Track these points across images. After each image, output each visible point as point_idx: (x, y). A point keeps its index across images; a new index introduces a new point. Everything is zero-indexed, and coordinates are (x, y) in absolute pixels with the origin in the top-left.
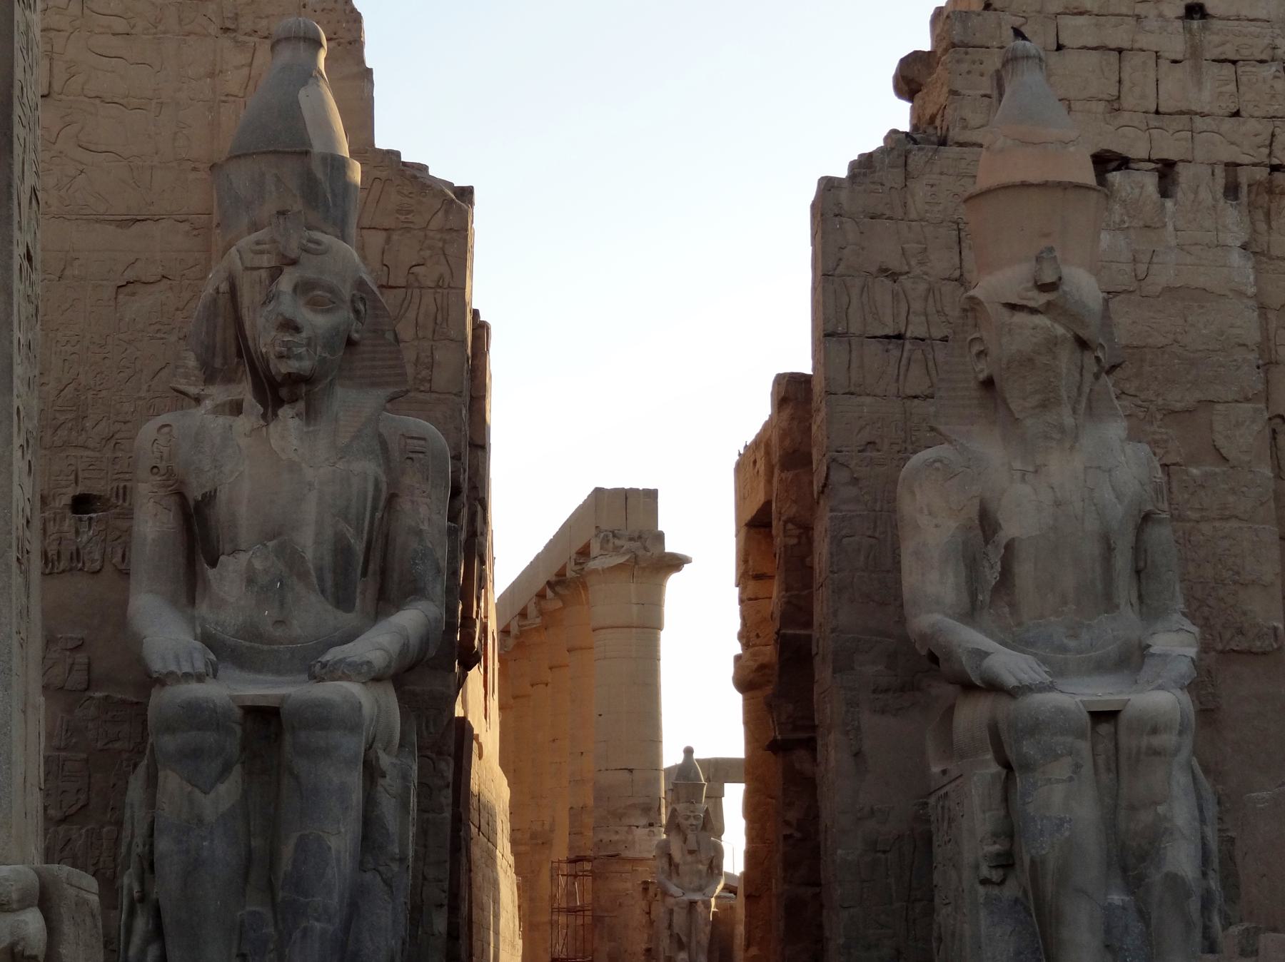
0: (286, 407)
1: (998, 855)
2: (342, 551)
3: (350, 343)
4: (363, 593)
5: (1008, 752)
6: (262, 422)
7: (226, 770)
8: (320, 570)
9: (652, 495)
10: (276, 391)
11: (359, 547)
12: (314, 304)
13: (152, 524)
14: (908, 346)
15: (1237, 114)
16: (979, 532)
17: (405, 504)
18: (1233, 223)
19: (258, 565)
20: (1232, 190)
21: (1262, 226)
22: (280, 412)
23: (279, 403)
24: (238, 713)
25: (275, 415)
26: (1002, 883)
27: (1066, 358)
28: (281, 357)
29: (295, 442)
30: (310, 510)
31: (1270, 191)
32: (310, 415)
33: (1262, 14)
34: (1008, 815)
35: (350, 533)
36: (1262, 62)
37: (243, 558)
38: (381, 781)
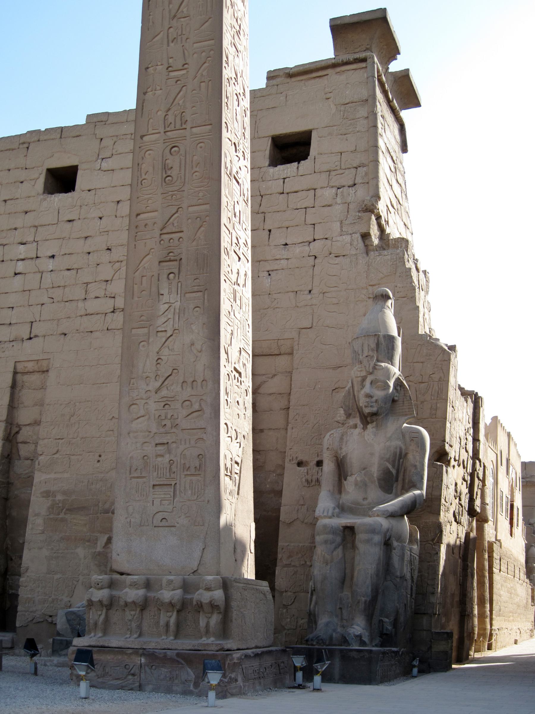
0: (370, 425)
3: (394, 401)
6: (362, 430)
7: (335, 548)
10: (367, 419)
11: (394, 472)
13: (329, 467)
17: (410, 456)
19: (358, 479)
22: (368, 426)
23: (368, 423)
24: (342, 528)
25: (367, 428)
29: (373, 436)
30: (376, 460)
32: (377, 426)
35: (390, 467)
37: (354, 477)
38: (393, 551)
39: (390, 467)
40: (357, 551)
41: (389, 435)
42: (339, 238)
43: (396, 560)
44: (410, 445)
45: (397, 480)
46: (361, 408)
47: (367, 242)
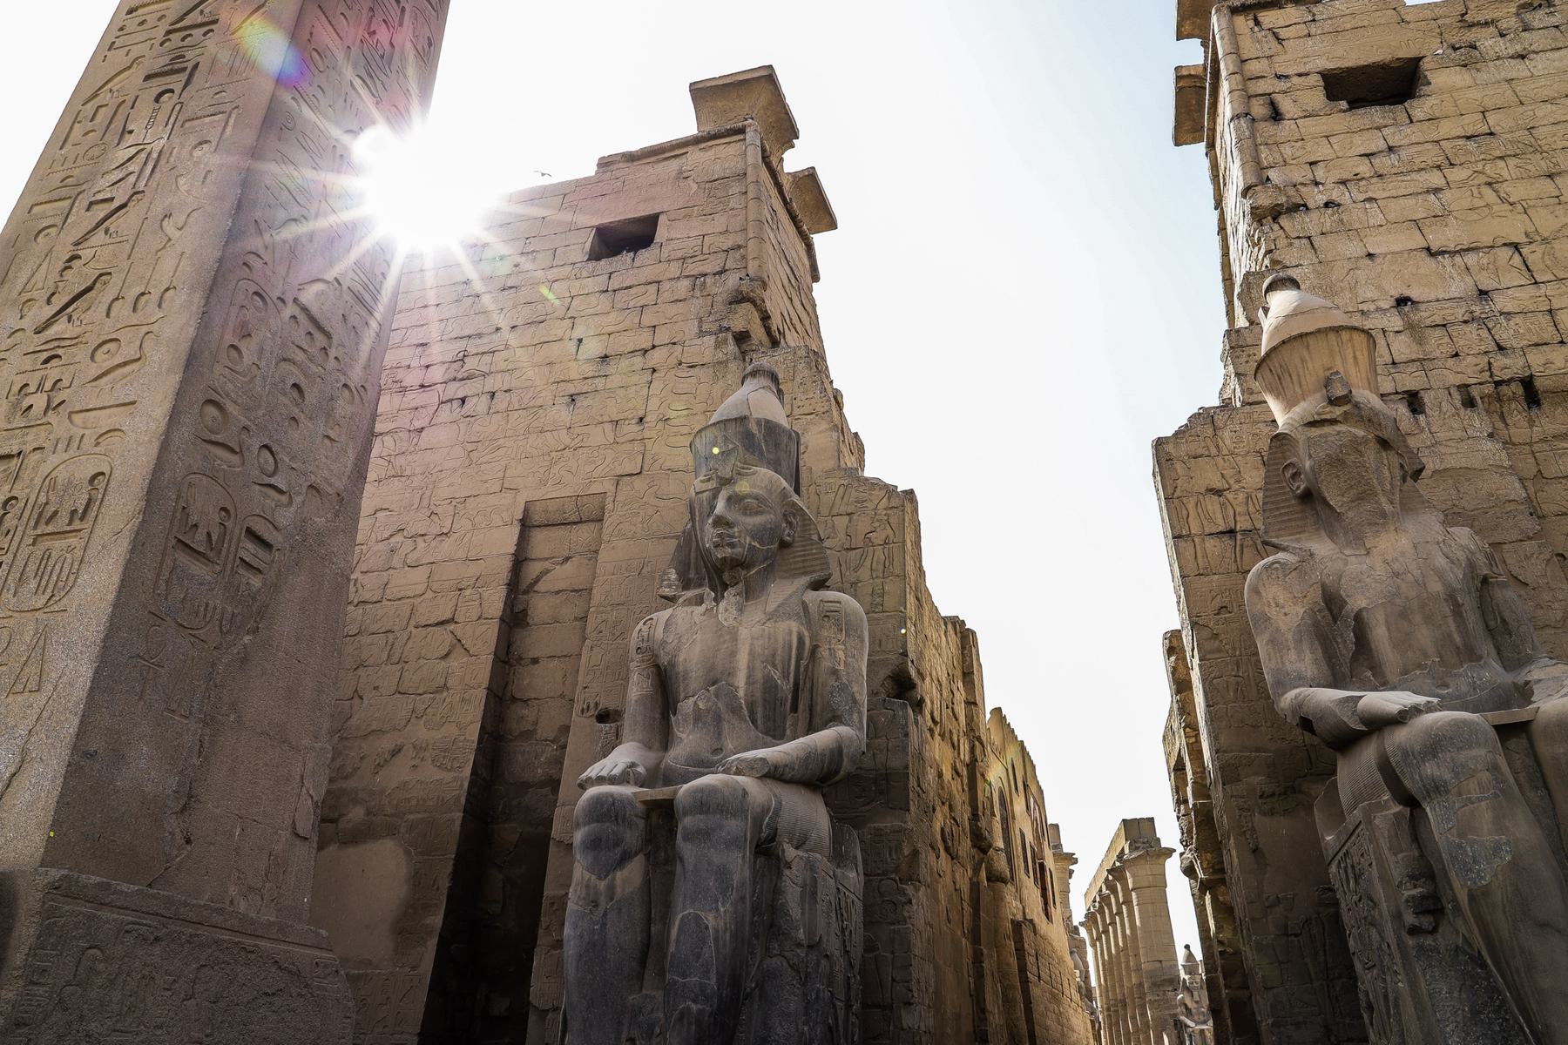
1: (1423, 897)
2: (769, 687)
4: (795, 725)
5: (1407, 783)
8: (751, 707)
9: (1151, 820)
11: (786, 687)
12: (747, 511)
13: (638, 688)
14: (1239, 537)
15: (1457, 355)
16: (1326, 613)
17: (824, 652)
18: (1478, 423)
19: (701, 706)
20: (1469, 403)
21: (1500, 425)
23: (725, 587)
24: (640, 807)
26: (1434, 931)
27: (1371, 454)
28: (717, 546)
30: (743, 660)
31: (1500, 400)
33: (1456, 295)
34: (1422, 856)
35: (777, 675)
36: (1465, 322)
38: (787, 872)
39: (777, 675)
40: (679, 867)
41: (771, 607)
42: (699, 341)
43: (792, 894)
44: (822, 627)
45: (795, 709)
46: (708, 551)
47: (744, 347)
